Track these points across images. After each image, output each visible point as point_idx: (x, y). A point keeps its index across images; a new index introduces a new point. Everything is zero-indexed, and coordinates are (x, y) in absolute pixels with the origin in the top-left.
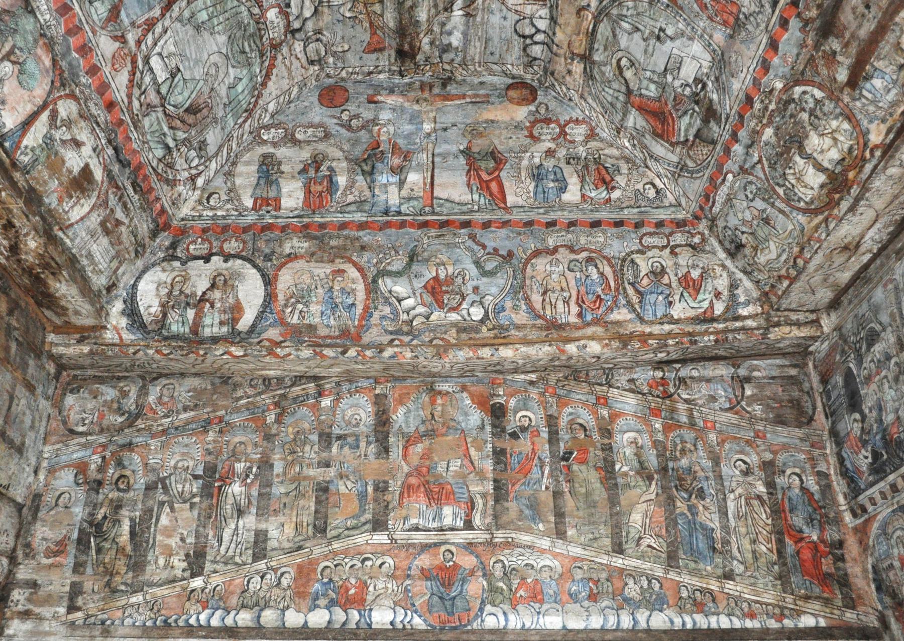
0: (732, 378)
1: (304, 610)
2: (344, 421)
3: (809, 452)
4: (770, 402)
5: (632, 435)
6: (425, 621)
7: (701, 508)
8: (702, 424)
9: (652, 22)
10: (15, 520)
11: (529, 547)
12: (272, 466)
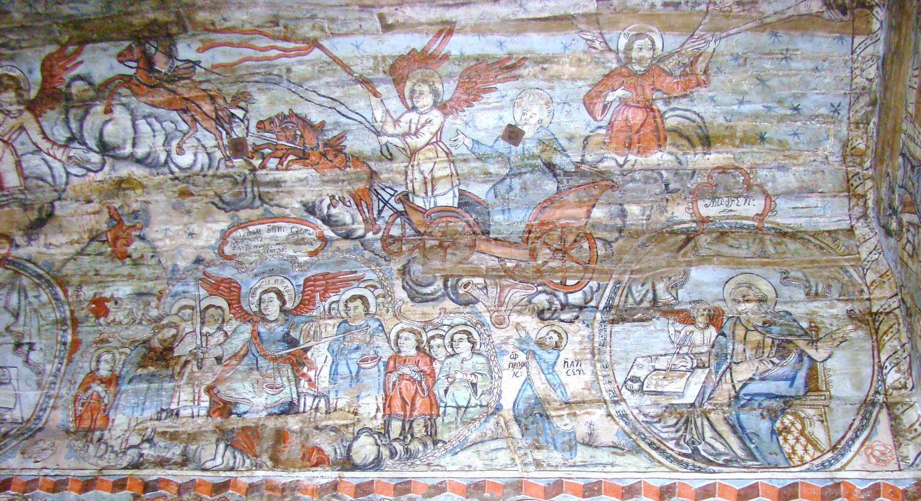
9: (34, 331)
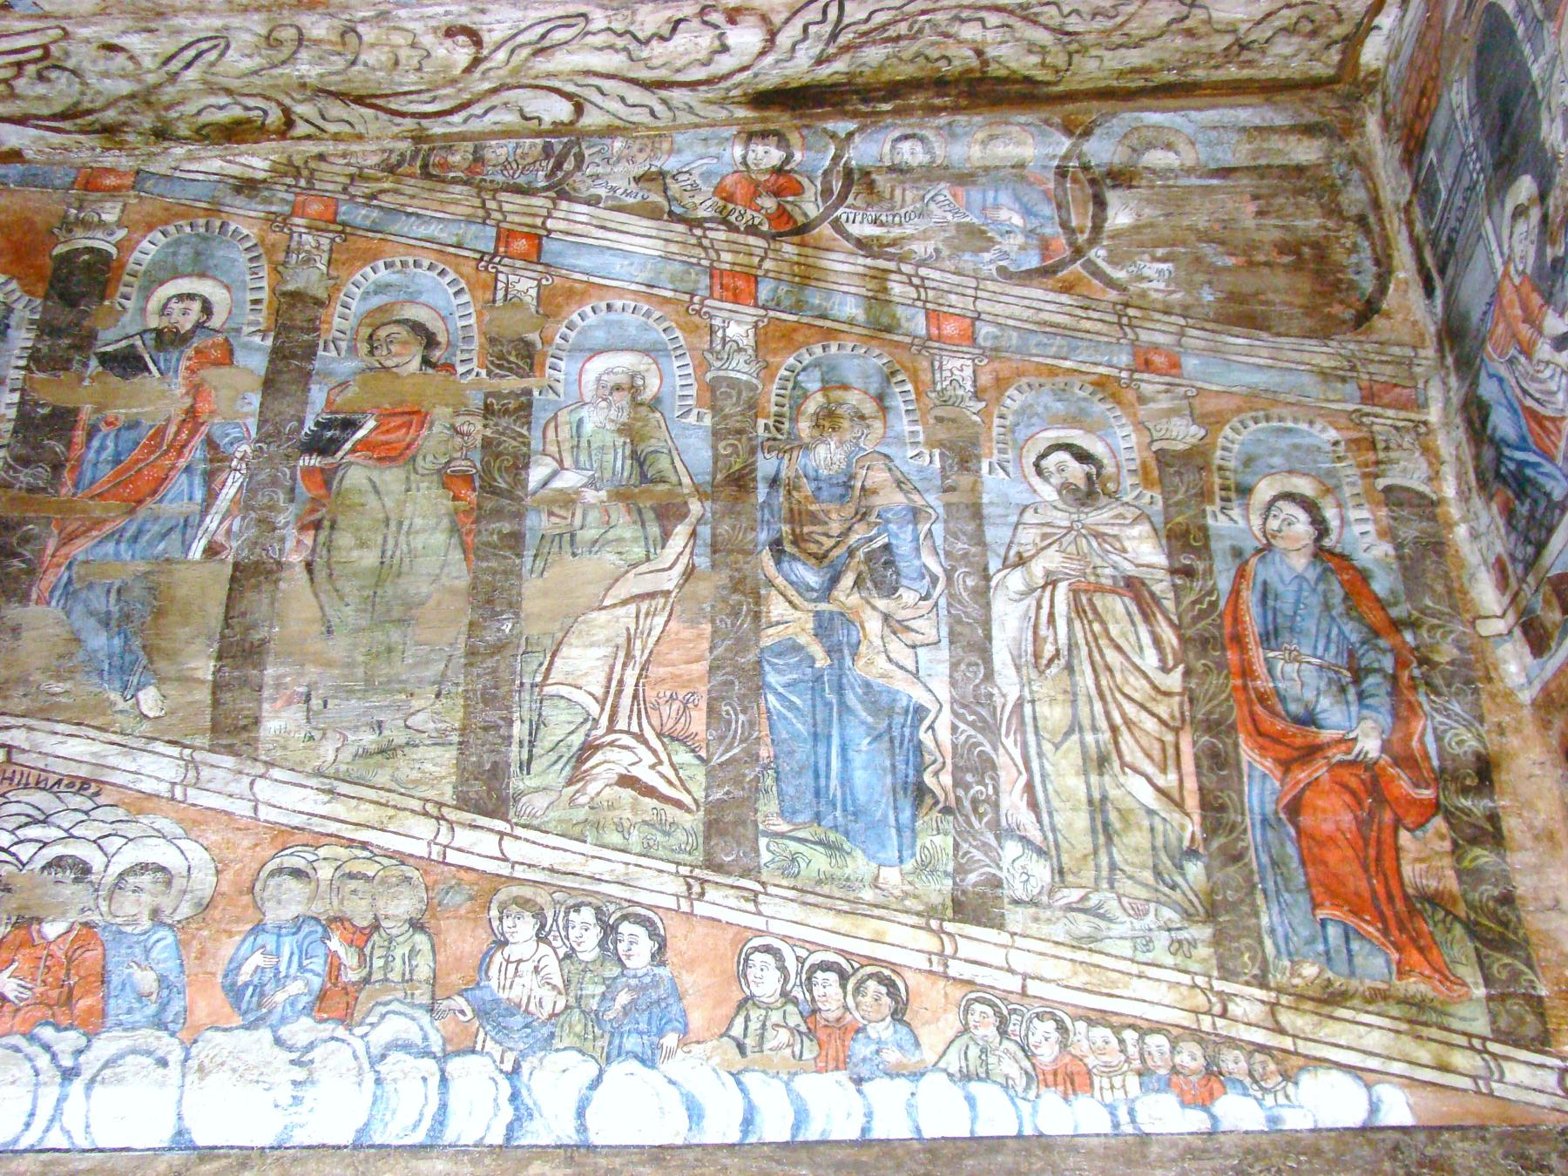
0: (1062, 172)
3: (1355, 419)
4: (1207, 249)
5: (625, 361)
7: (874, 625)
8: (920, 325)
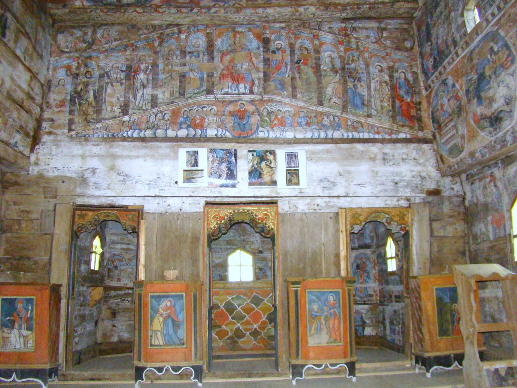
0: (378, 28)
1: (176, 130)
2: (192, 45)
3: (410, 63)
5: (330, 53)
6: (231, 134)
7: (359, 86)
10: (41, 91)
11: (280, 102)
12: (158, 66)
